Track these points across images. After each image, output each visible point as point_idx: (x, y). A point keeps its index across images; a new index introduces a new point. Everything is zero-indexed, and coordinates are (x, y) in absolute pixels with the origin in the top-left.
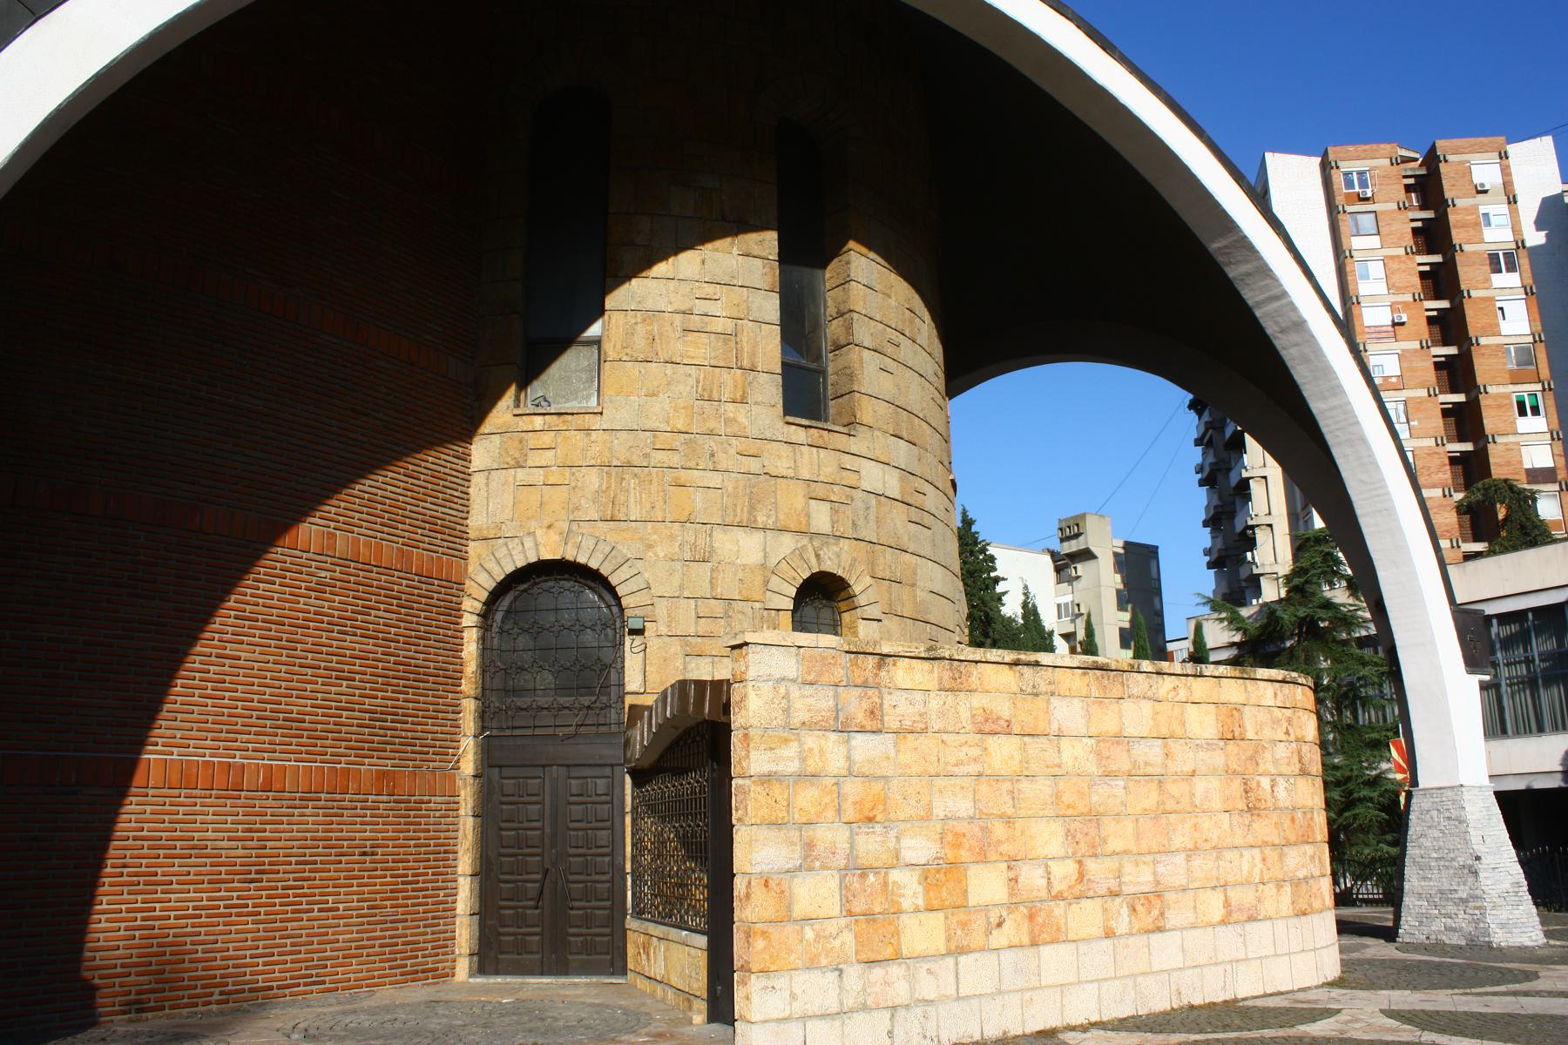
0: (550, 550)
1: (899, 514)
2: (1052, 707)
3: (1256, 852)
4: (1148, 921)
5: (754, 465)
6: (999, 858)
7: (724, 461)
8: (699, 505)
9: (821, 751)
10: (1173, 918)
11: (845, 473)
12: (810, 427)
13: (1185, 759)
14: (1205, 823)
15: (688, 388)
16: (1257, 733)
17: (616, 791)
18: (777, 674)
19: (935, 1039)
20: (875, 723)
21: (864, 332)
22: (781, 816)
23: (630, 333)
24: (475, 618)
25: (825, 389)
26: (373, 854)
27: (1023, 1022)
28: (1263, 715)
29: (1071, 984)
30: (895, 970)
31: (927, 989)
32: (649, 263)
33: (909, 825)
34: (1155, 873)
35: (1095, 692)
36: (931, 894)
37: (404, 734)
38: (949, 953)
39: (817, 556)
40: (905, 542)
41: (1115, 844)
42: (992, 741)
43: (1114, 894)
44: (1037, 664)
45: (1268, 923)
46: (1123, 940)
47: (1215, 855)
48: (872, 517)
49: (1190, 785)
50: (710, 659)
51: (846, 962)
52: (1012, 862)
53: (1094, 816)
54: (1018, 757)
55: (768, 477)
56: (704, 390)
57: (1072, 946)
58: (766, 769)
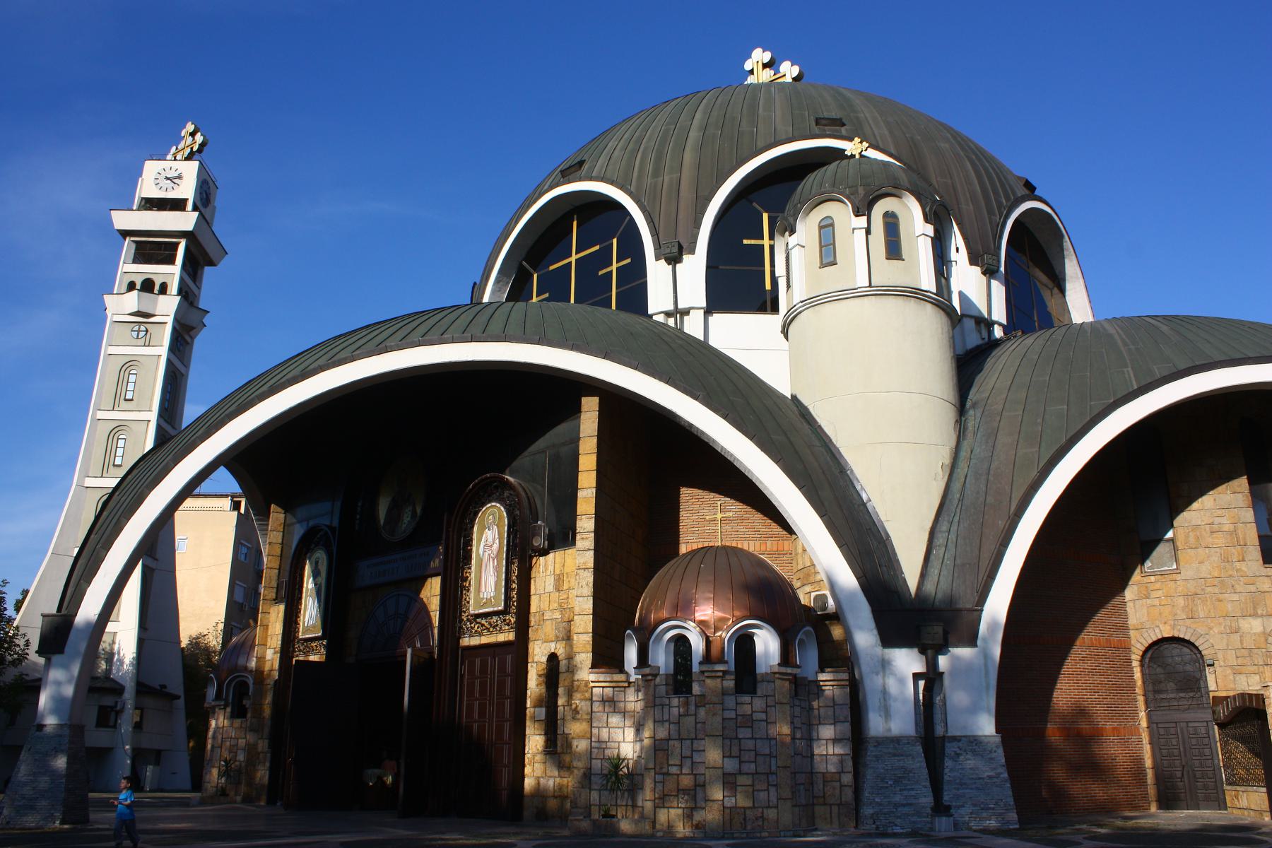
0: (1167, 634)
5: (1252, 588)
7: (1238, 588)
8: (1230, 609)
17: (1211, 732)
23: (1187, 537)
24: (1138, 663)
50: (1245, 675)
56: (1224, 557)
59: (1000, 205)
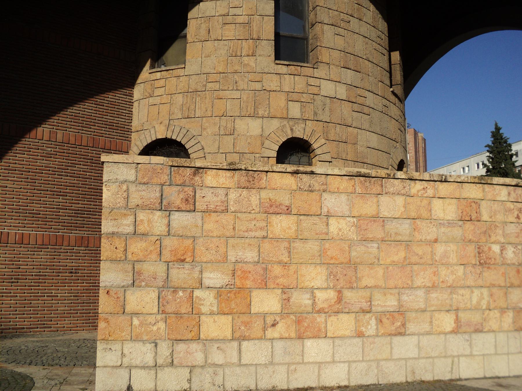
1: (346, 109)
2: (323, 199)
3: (485, 291)
4: (392, 329)
5: (258, 86)
6: (276, 286)
7: (242, 85)
9: (149, 221)
10: (411, 327)
11: (310, 87)
12: (290, 65)
15: (225, 51)
16: (491, 217)
18: (121, 178)
19: (222, 387)
21: (323, 16)
22: (119, 256)
23: (199, 28)
25: (307, 47)
26: (76, 273)
27: (288, 382)
28: (496, 206)
29: (328, 362)
30: (194, 346)
31: (217, 358)
33: (209, 265)
34: (399, 300)
35: (358, 190)
36: (223, 305)
37: (93, 220)
38: (233, 339)
39: (292, 130)
40: (349, 121)
42: (275, 219)
43: (364, 312)
44: (312, 173)
45: (491, 336)
46: (371, 339)
47: (449, 291)
48: (327, 109)
49: (432, 248)
51: (160, 339)
52: (285, 289)
54: (294, 228)
55: (266, 91)
56: (233, 51)
57: (331, 341)
58: (111, 230)
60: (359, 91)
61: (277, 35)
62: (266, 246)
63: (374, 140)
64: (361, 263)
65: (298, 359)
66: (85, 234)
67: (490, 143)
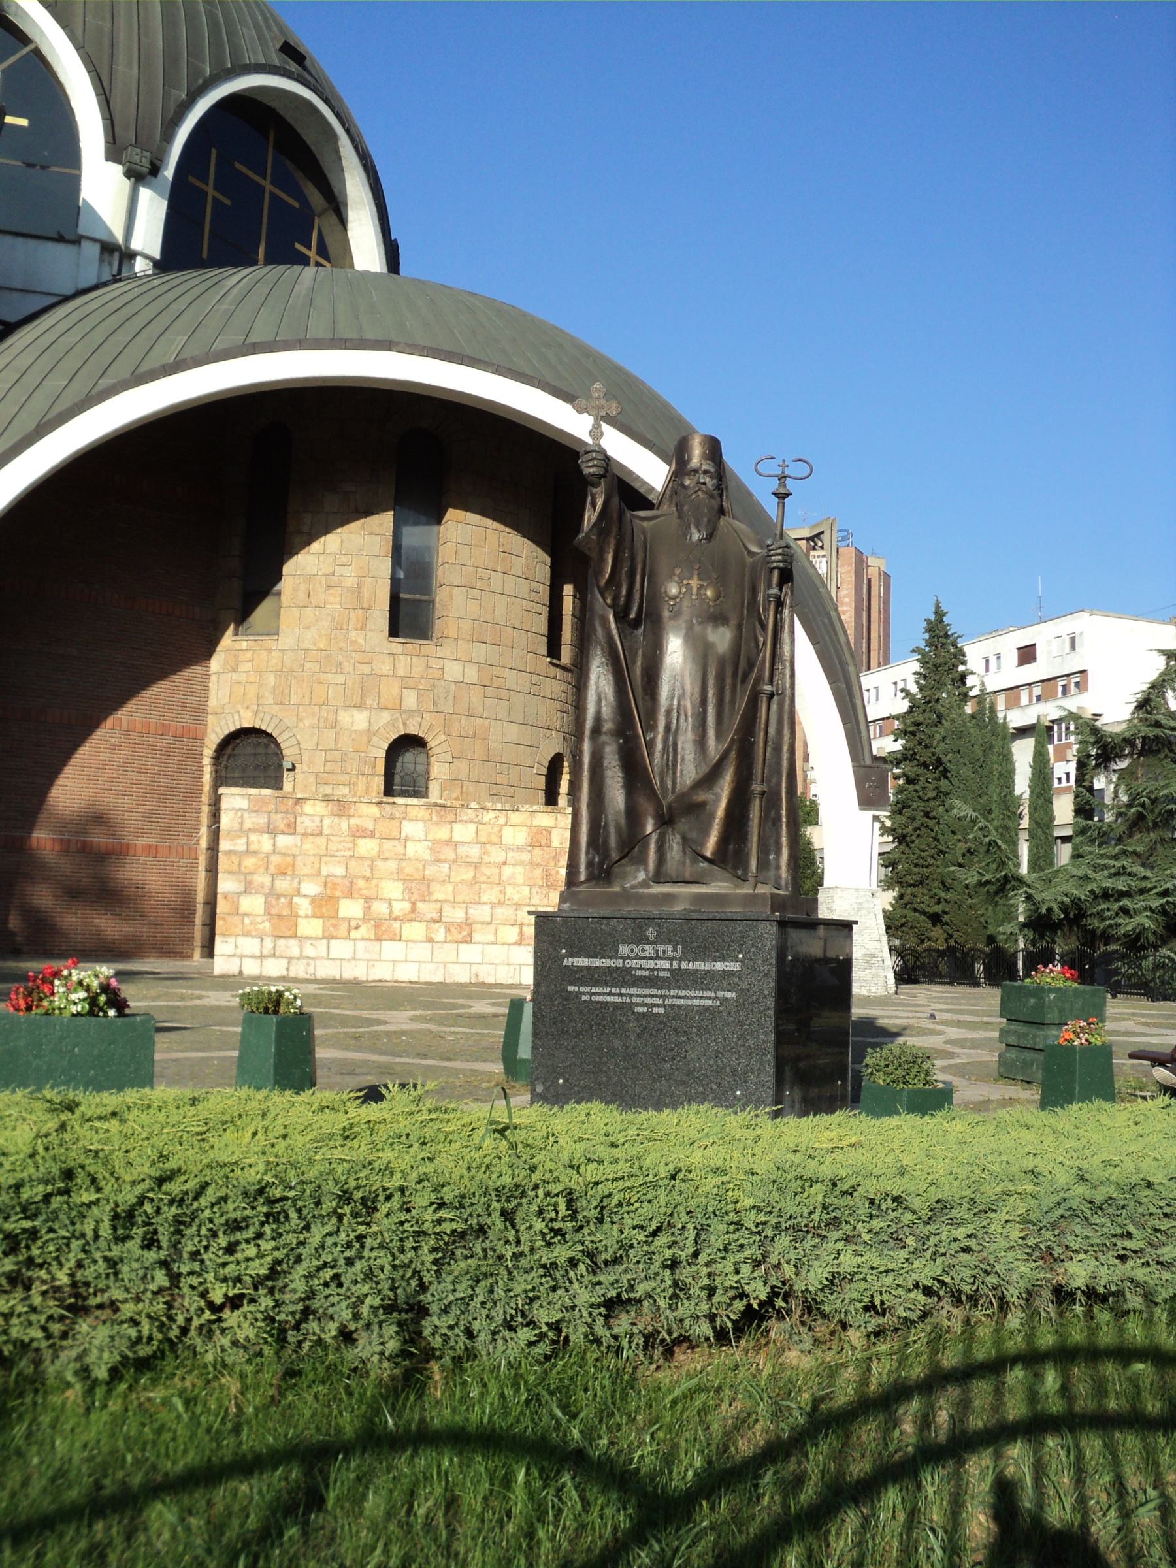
1: (476, 695)
5: (366, 669)
7: (347, 667)
9: (259, 842)
10: (477, 937)
13: (497, 855)
14: (509, 891)
18: (237, 807)
20: (292, 829)
23: (296, 589)
30: (293, 943)
31: (309, 951)
32: (309, 543)
35: (434, 818)
38: (323, 938)
39: (405, 724)
41: (436, 896)
43: (435, 921)
48: (451, 697)
52: (367, 899)
53: (426, 882)
59: (194, 72)
60: (495, 671)
61: (395, 600)
62: (353, 863)
63: (513, 732)
64: (433, 880)
65: (377, 957)
66: (153, 842)
67: (922, 645)
